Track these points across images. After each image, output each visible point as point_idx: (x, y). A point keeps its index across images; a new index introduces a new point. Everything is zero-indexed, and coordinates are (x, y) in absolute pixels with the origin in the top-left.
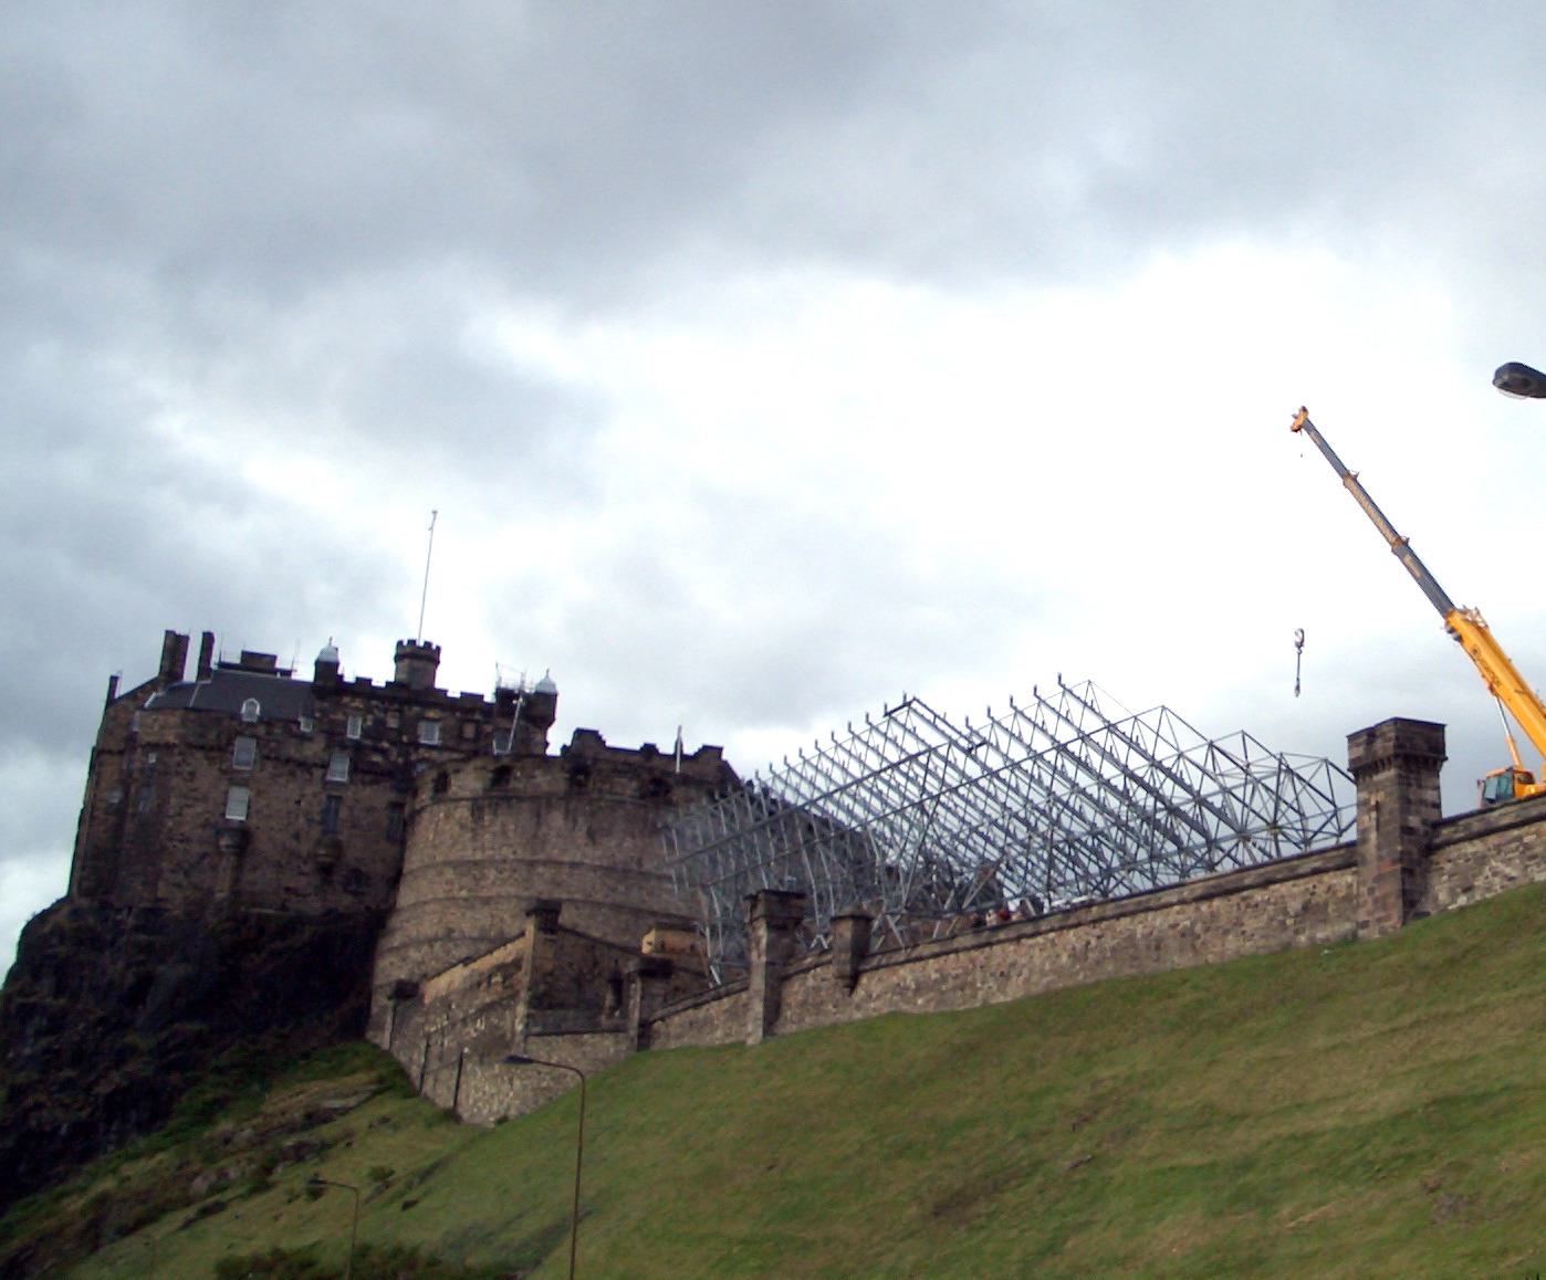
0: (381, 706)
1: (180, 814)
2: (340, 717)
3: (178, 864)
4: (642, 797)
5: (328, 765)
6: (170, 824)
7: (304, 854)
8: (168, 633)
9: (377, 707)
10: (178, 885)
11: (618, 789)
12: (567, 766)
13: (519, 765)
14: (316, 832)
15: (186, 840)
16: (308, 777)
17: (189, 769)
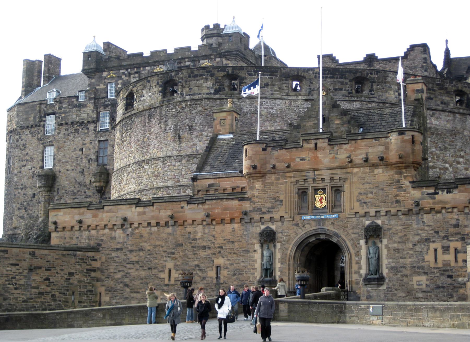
0: (126, 72)
1: (20, 172)
2: (102, 86)
3: (21, 204)
4: (217, 92)
5: (98, 120)
6: (16, 179)
7: (88, 182)
8: (24, 60)
9: (124, 74)
10: (22, 217)
11: (195, 90)
12: (160, 83)
13: (135, 89)
14: (94, 167)
15: (24, 188)
16: (86, 131)
17: (22, 142)
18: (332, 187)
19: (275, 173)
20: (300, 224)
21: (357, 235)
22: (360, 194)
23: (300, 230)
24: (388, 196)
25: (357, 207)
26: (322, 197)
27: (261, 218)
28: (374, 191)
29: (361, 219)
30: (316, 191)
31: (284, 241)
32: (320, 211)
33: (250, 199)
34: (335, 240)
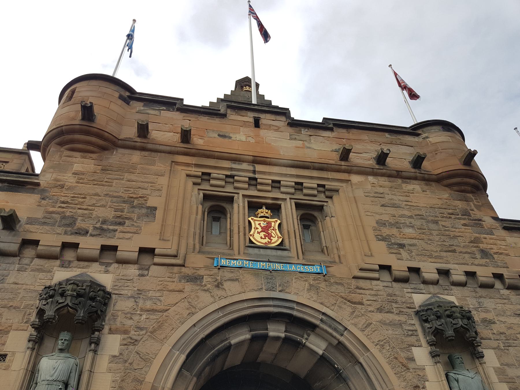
18: (298, 206)
19: (143, 149)
20: (206, 279)
21: (398, 331)
22: (381, 223)
23: (205, 297)
24: (455, 237)
25: (382, 255)
26: (269, 224)
27: (65, 246)
28: (418, 223)
29: (397, 286)
30: (253, 207)
31: (141, 329)
32: (269, 252)
33: (44, 190)
34: (317, 345)
